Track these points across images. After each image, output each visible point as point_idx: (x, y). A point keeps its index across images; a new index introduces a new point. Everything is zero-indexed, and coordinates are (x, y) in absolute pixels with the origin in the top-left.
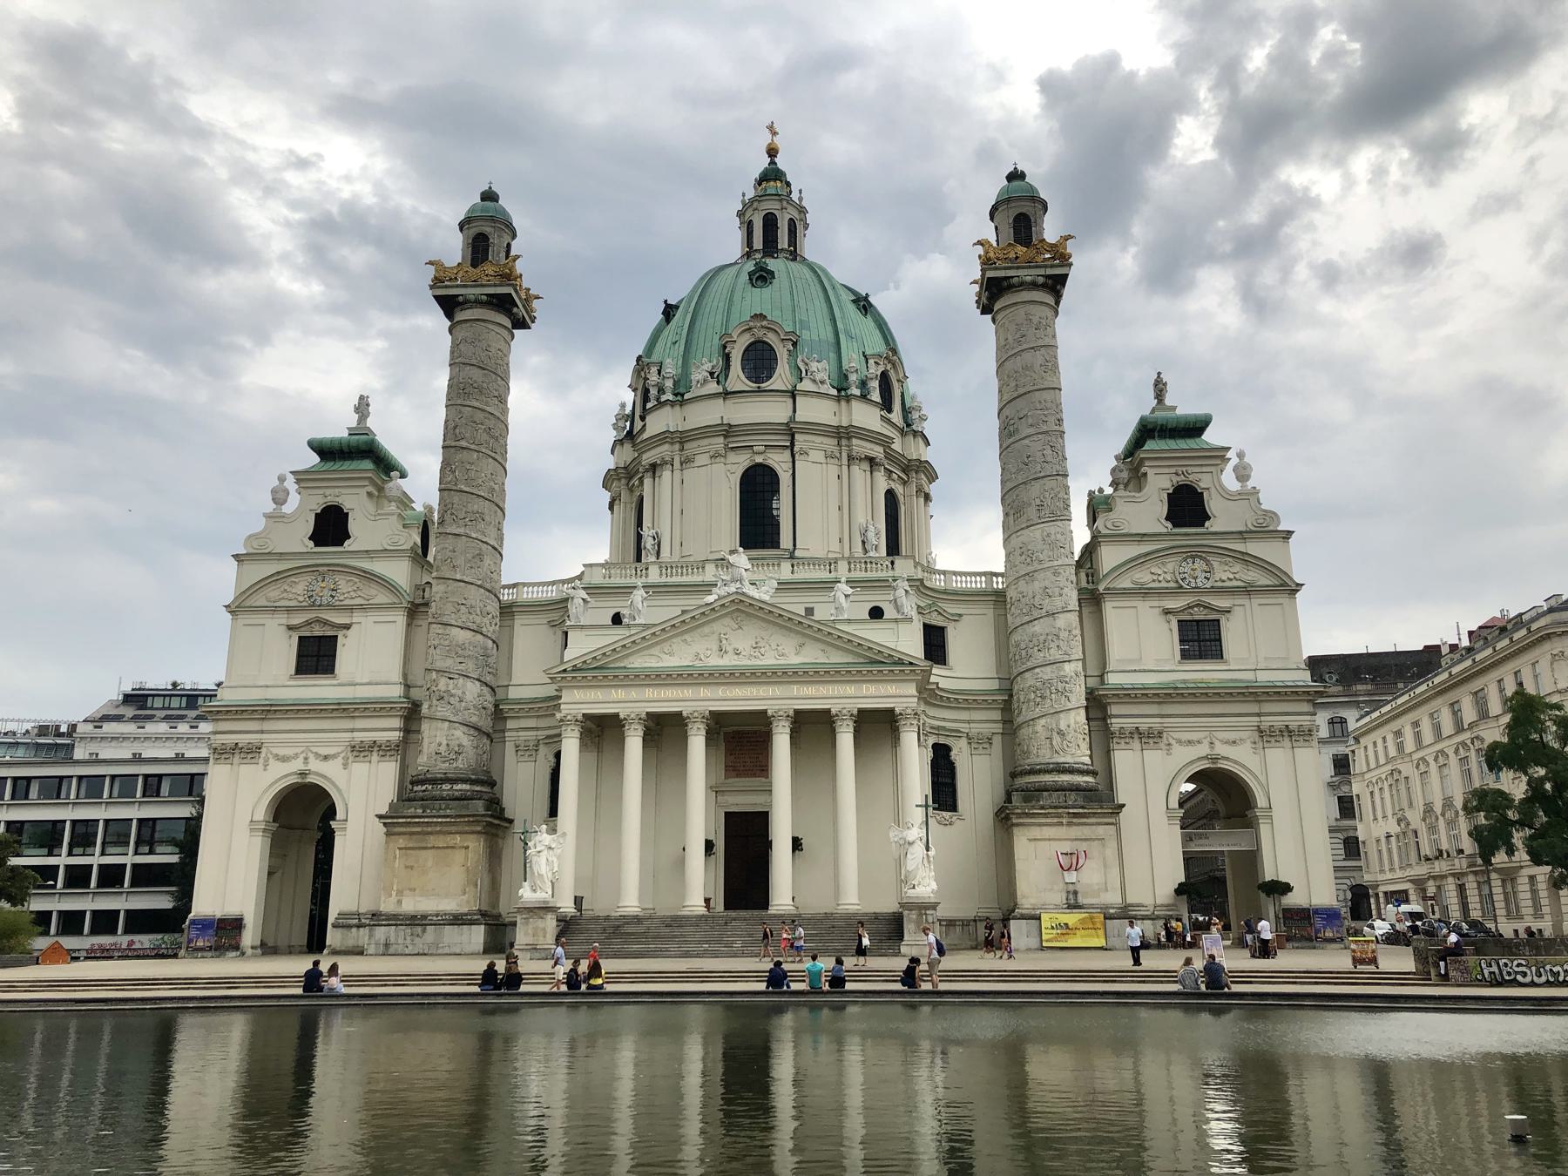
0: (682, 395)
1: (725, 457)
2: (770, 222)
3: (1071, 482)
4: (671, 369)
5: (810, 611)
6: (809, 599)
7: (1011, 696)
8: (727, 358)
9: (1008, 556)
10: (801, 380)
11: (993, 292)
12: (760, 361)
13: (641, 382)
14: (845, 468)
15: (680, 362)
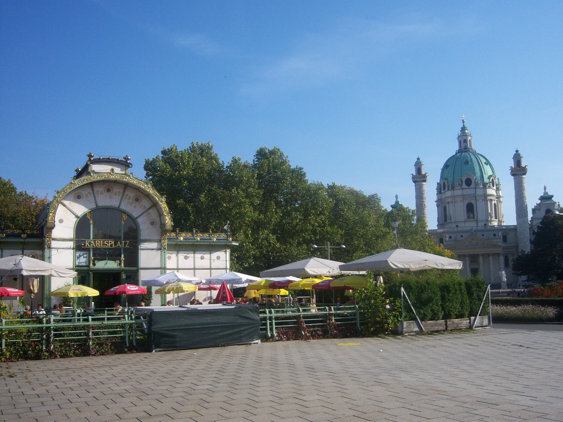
0: (454, 188)
1: (463, 201)
2: (465, 141)
3: (528, 210)
4: (450, 183)
5: (483, 235)
6: (483, 233)
7: (518, 247)
8: (462, 181)
9: (517, 223)
10: (477, 185)
11: (513, 175)
12: (469, 182)
13: (443, 182)
14: (486, 202)
15: (452, 181)
